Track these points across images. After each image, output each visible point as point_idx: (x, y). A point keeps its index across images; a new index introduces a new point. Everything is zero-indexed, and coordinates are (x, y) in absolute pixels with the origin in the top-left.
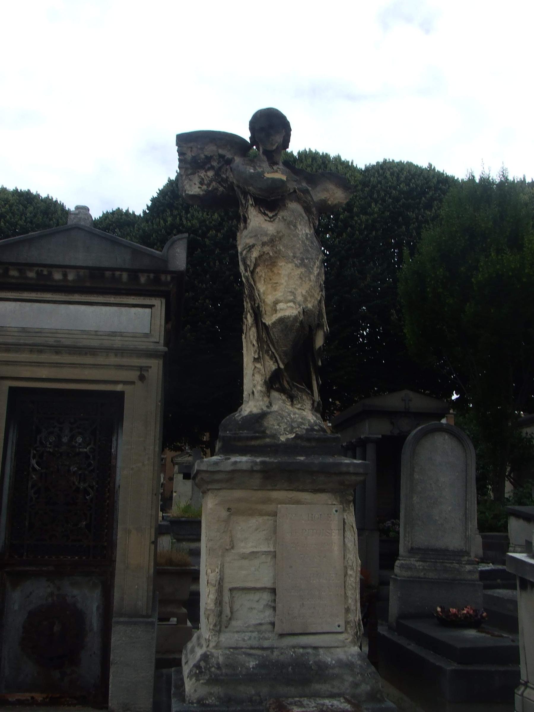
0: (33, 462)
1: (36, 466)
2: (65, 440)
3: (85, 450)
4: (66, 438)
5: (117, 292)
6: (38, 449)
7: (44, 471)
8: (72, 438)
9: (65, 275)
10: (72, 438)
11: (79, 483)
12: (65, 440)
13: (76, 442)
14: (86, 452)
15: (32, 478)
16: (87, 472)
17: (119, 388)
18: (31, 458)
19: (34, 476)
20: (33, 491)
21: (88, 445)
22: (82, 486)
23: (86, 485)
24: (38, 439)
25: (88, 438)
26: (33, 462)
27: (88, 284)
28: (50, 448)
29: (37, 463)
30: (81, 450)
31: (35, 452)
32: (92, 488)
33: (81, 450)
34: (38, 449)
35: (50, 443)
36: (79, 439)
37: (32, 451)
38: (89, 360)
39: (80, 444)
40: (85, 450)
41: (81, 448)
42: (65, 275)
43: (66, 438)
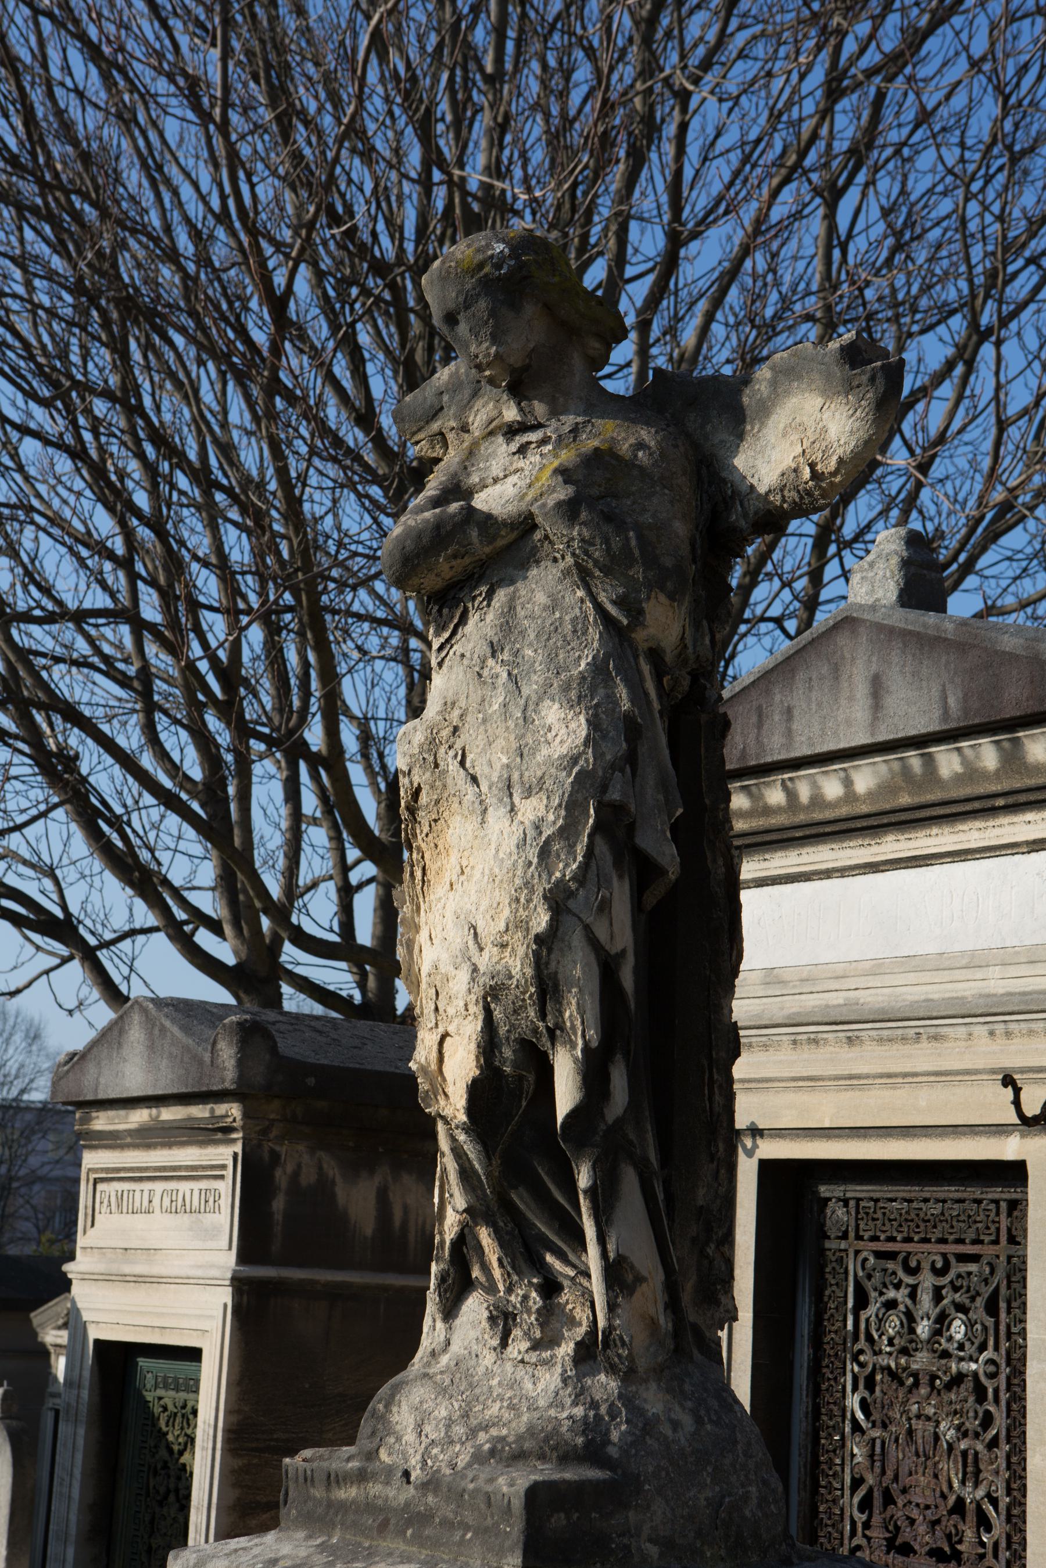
0: (853, 1402)
1: (860, 1416)
2: (923, 1329)
3: (974, 1366)
4: (925, 1322)
5: (984, 807)
6: (862, 1358)
7: (876, 1433)
8: (942, 1321)
9: (848, 783)
10: (942, 1321)
11: (963, 1482)
12: (923, 1329)
13: (950, 1339)
14: (975, 1374)
15: (853, 1456)
16: (980, 1447)
17: (1009, 1148)
18: (849, 1388)
19: (856, 1450)
20: (856, 1500)
21: (983, 1348)
22: (972, 1494)
23: (980, 1493)
24: (863, 1326)
25: (978, 1326)
26: (853, 1402)
27: (905, 800)
28: (890, 1354)
29: (864, 1405)
30: (964, 1366)
31: (856, 1368)
32: (994, 1502)
33: (964, 1366)
34: (862, 1358)
35: (891, 1343)
36: (958, 1329)
37: (849, 1367)
38: (922, 1057)
39: (961, 1347)
40: (974, 1366)
41: (962, 1359)
42: (848, 783)
43: (925, 1322)
